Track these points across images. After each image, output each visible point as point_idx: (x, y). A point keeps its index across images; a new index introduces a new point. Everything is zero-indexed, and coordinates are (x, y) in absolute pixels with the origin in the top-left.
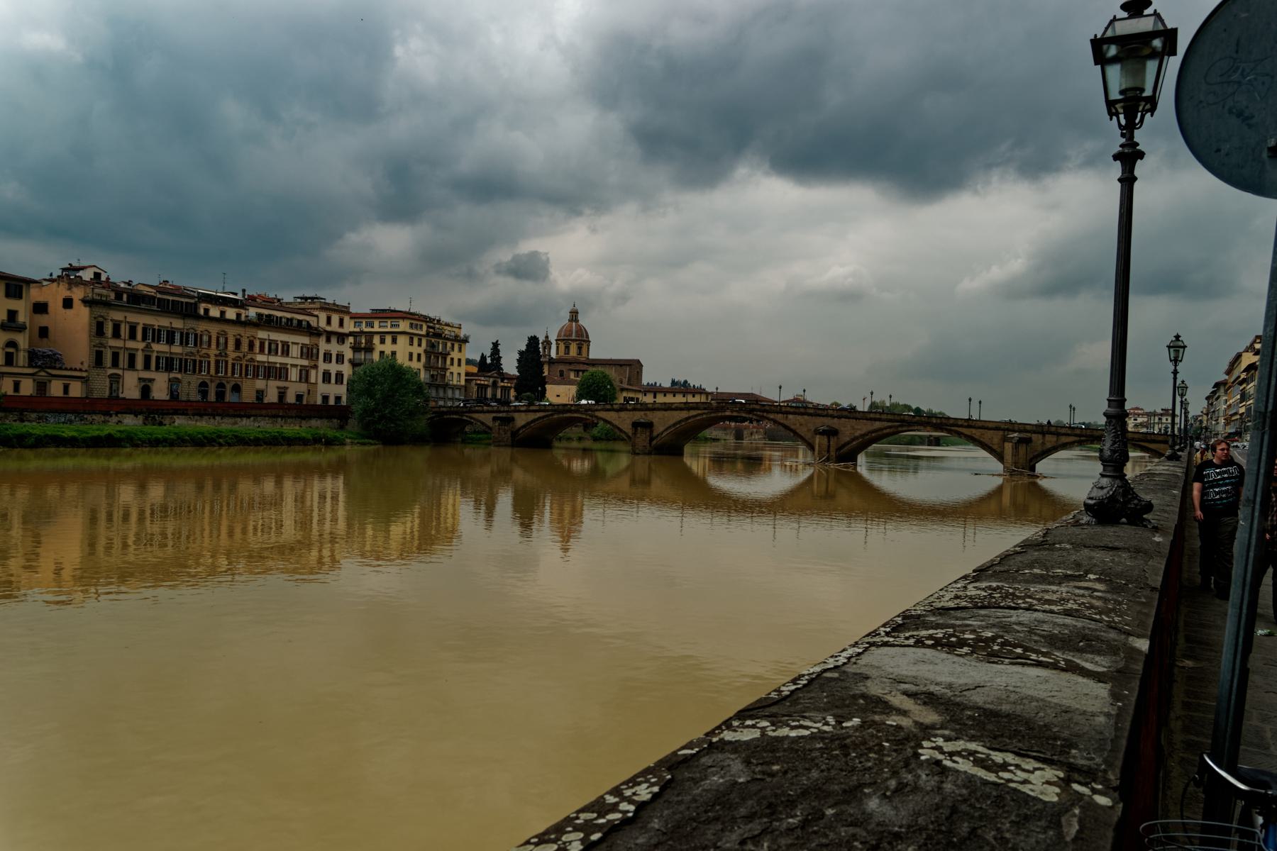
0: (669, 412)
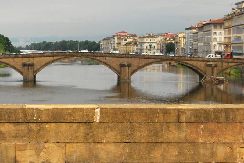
0: (43, 58)
